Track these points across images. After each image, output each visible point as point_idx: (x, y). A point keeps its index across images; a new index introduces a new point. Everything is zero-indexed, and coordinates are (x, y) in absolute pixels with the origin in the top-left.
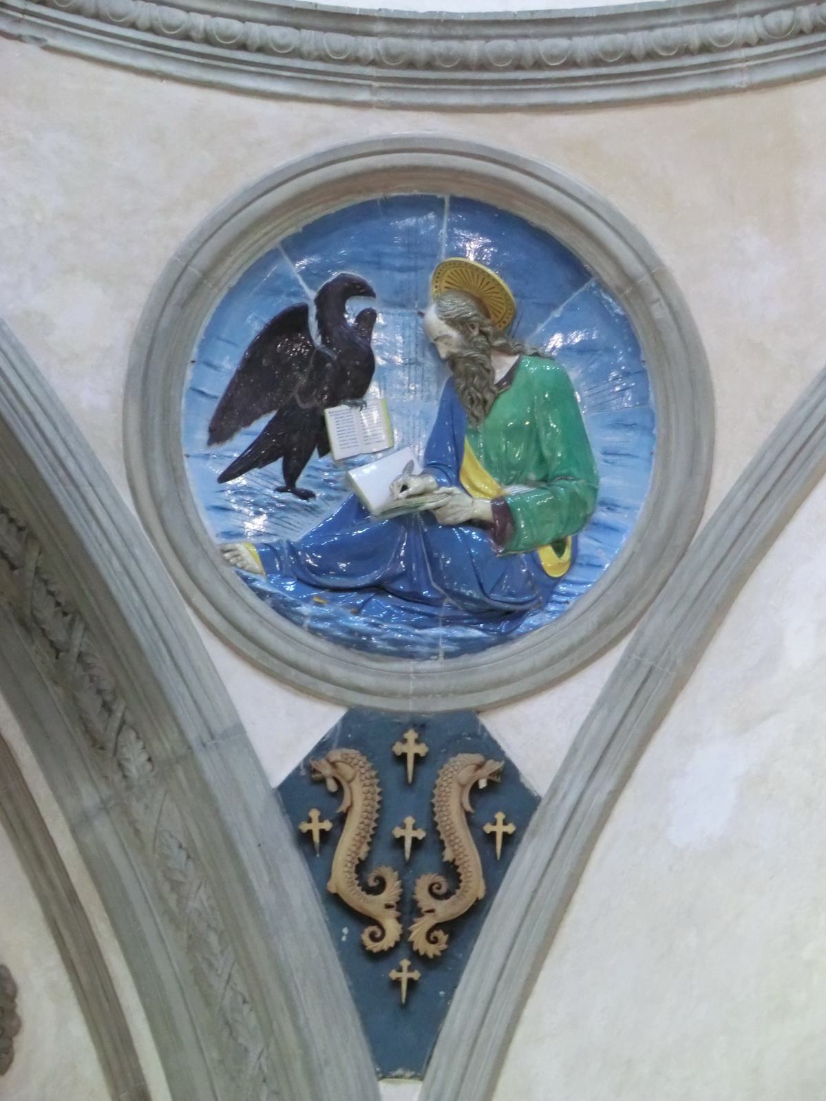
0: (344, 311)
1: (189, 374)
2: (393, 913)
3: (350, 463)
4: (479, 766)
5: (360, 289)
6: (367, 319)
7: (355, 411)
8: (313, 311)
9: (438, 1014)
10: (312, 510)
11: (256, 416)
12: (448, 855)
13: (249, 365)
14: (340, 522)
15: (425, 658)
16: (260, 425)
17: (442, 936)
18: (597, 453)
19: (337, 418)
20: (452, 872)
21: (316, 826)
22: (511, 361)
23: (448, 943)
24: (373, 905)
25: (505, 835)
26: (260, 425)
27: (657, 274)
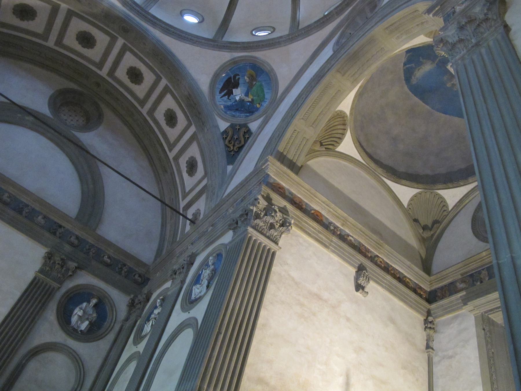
0: (236, 78)
1: (217, 86)
2: (232, 146)
3: (236, 95)
4: (246, 129)
5: (239, 75)
6: (239, 78)
7: (237, 90)
8: (232, 78)
9: (236, 158)
10: (231, 101)
11: (225, 90)
12: (240, 139)
13: (224, 84)
14: (234, 102)
15: (242, 118)
16: (225, 92)
17: (238, 149)
18: (265, 93)
19: (234, 90)
20: (240, 142)
21: (225, 136)
22: (255, 82)
23: (239, 149)
24: (230, 145)
25: (248, 137)
26: (225, 92)
27: (272, 69)
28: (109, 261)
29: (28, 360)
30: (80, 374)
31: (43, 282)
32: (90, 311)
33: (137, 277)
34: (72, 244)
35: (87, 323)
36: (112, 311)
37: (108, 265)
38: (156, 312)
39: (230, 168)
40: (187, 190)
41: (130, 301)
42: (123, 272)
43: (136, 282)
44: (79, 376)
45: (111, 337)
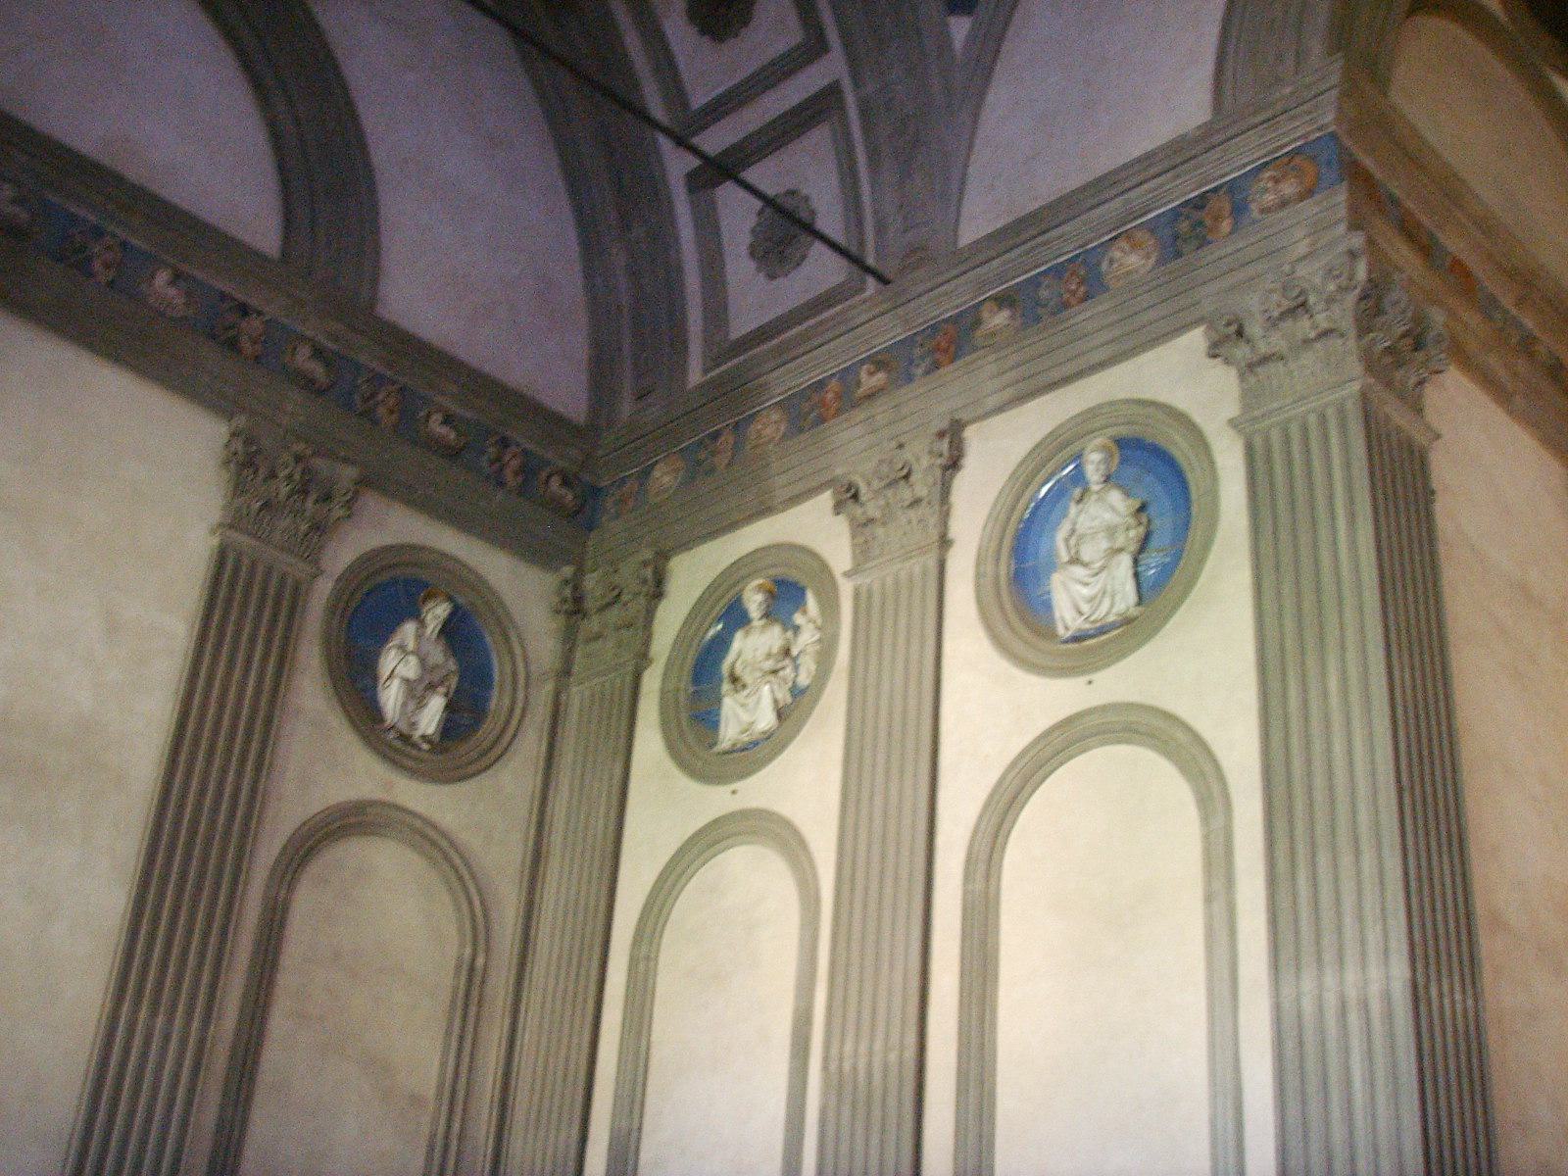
28: (452, 435)
29: (291, 888)
30: (470, 903)
31: (253, 564)
32: (437, 654)
33: (555, 483)
34: (308, 383)
35: (436, 705)
36: (507, 639)
37: (453, 454)
38: (752, 647)
39: (960, 28)
40: (699, 99)
41: (568, 592)
42: (508, 474)
43: (555, 505)
44: (465, 906)
45: (530, 744)
